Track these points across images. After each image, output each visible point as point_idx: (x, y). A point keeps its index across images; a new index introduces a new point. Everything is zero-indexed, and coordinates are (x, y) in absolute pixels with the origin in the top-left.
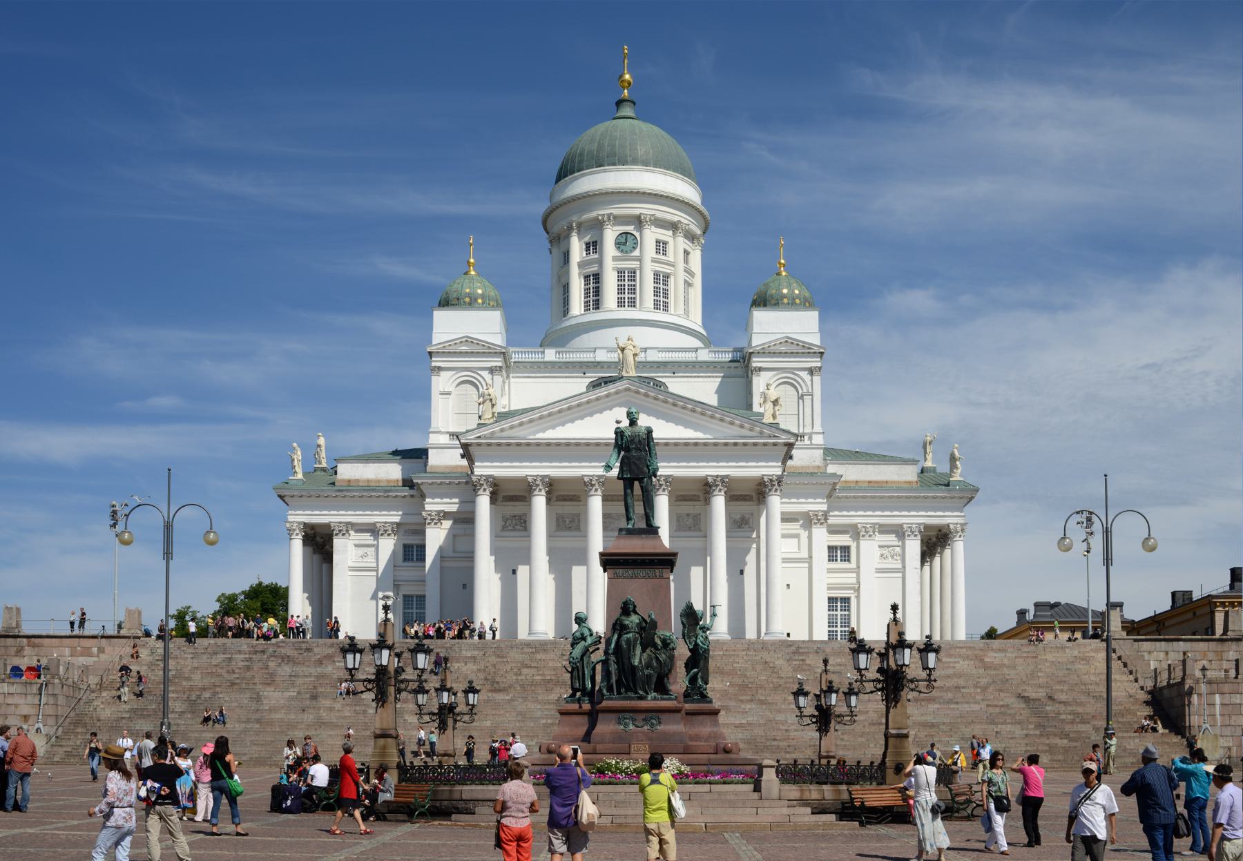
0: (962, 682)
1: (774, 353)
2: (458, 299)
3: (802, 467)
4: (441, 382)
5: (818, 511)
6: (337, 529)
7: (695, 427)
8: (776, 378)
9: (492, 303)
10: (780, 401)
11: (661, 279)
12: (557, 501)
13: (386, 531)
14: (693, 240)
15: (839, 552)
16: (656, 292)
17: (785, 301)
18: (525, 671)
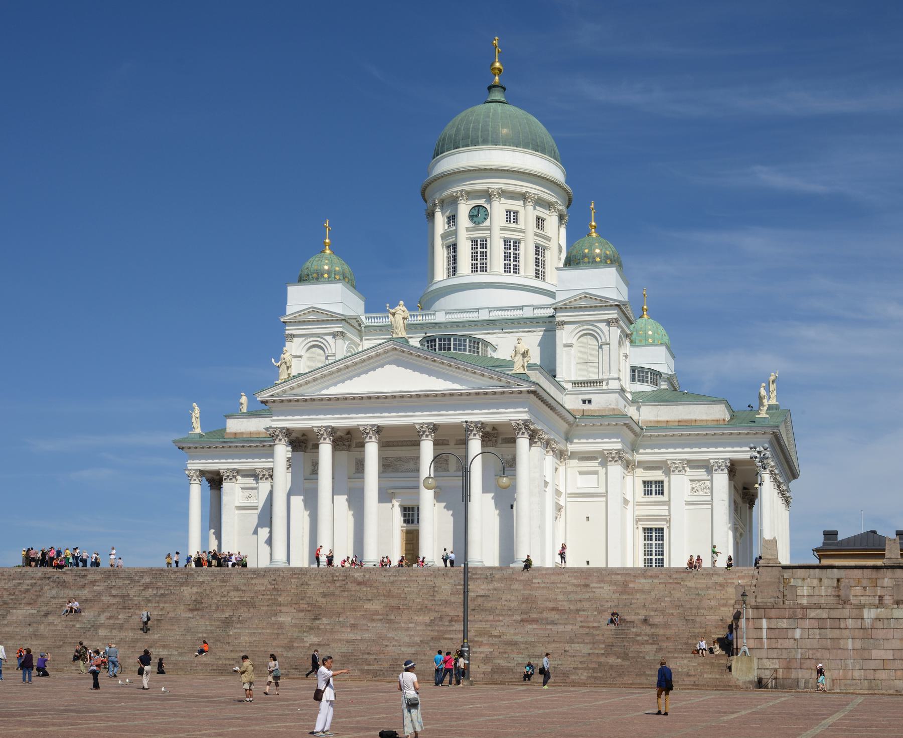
0: (586, 605)
1: (575, 308)
2: (308, 275)
3: (599, 410)
4: (293, 348)
5: (611, 450)
6: (226, 474)
7: (453, 380)
8: (578, 330)
9: (337, 277)
10: (530, 353)
11: (512, 246)
12: (356, 447)
13: (264, 475)
14: (550, 207)
15: (654, 486)
16: (507, 256)
17: (586, 260)
18: (232, 594)
